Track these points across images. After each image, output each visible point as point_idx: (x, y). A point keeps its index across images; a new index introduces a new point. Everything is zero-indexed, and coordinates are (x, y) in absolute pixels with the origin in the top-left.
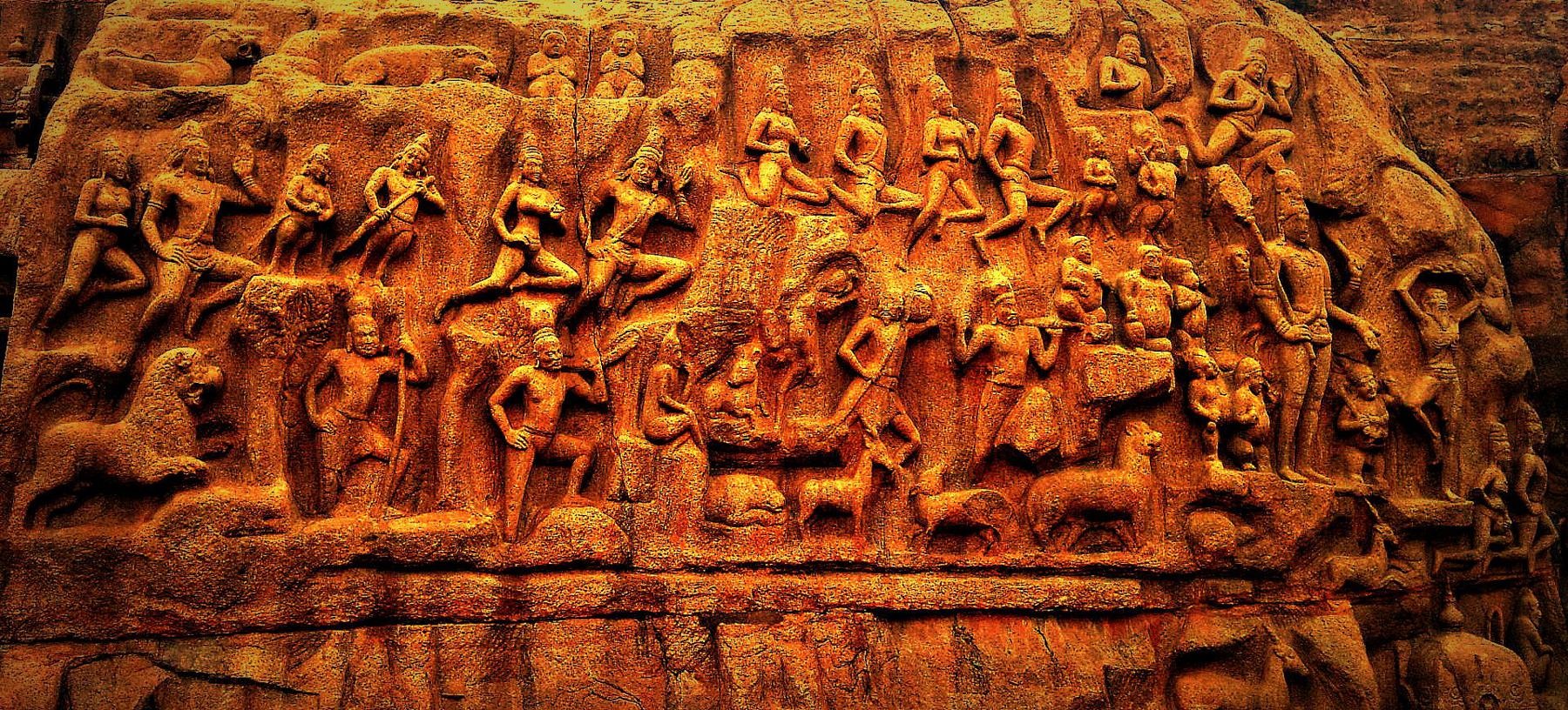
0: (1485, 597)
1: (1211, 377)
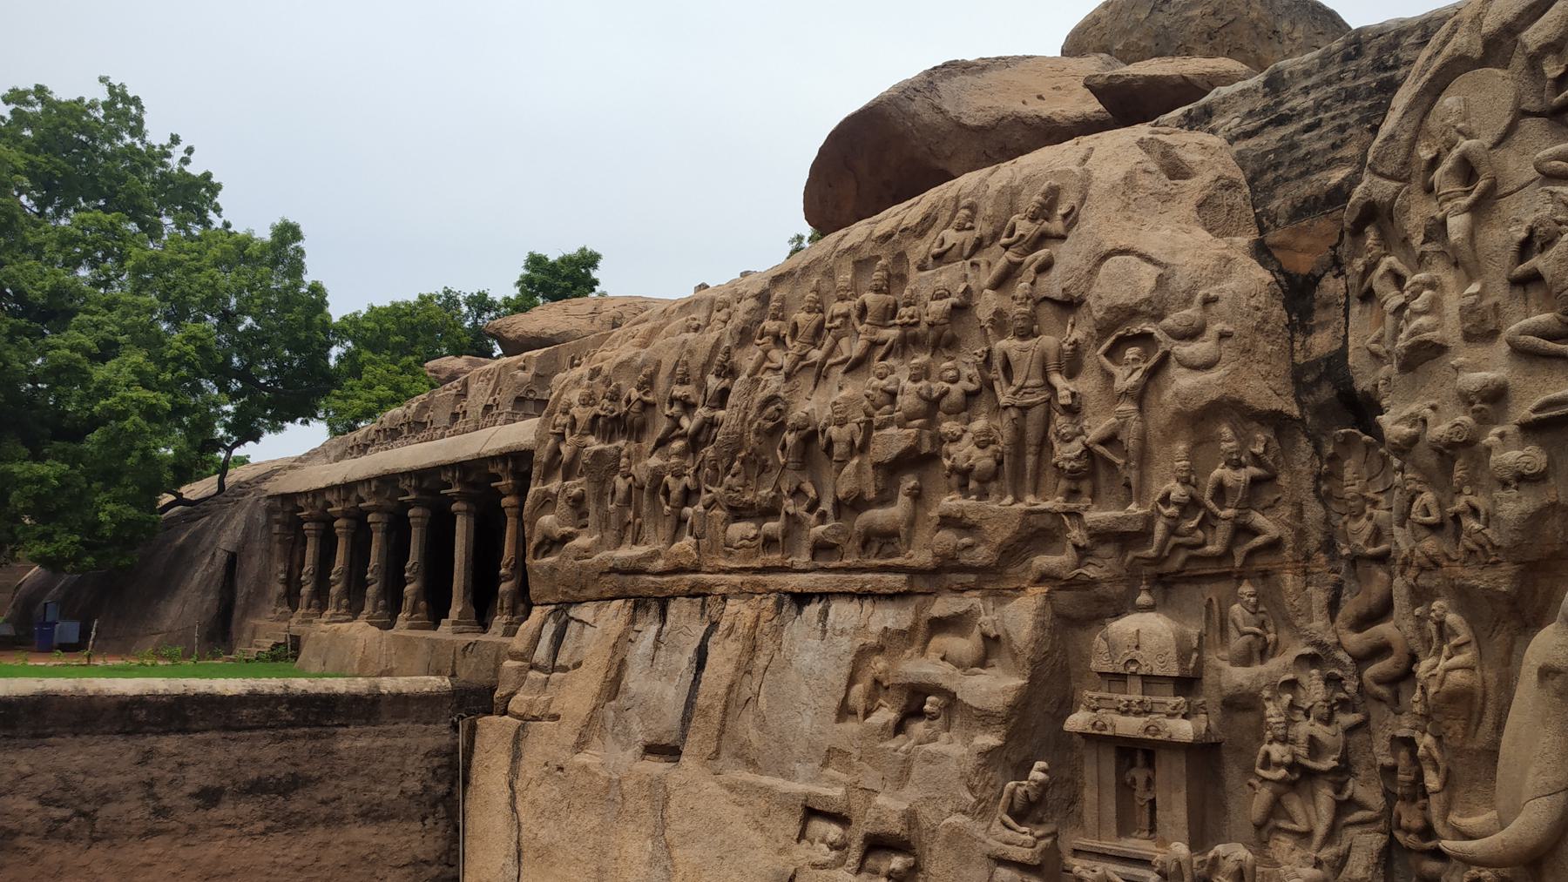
1: (952, 441)
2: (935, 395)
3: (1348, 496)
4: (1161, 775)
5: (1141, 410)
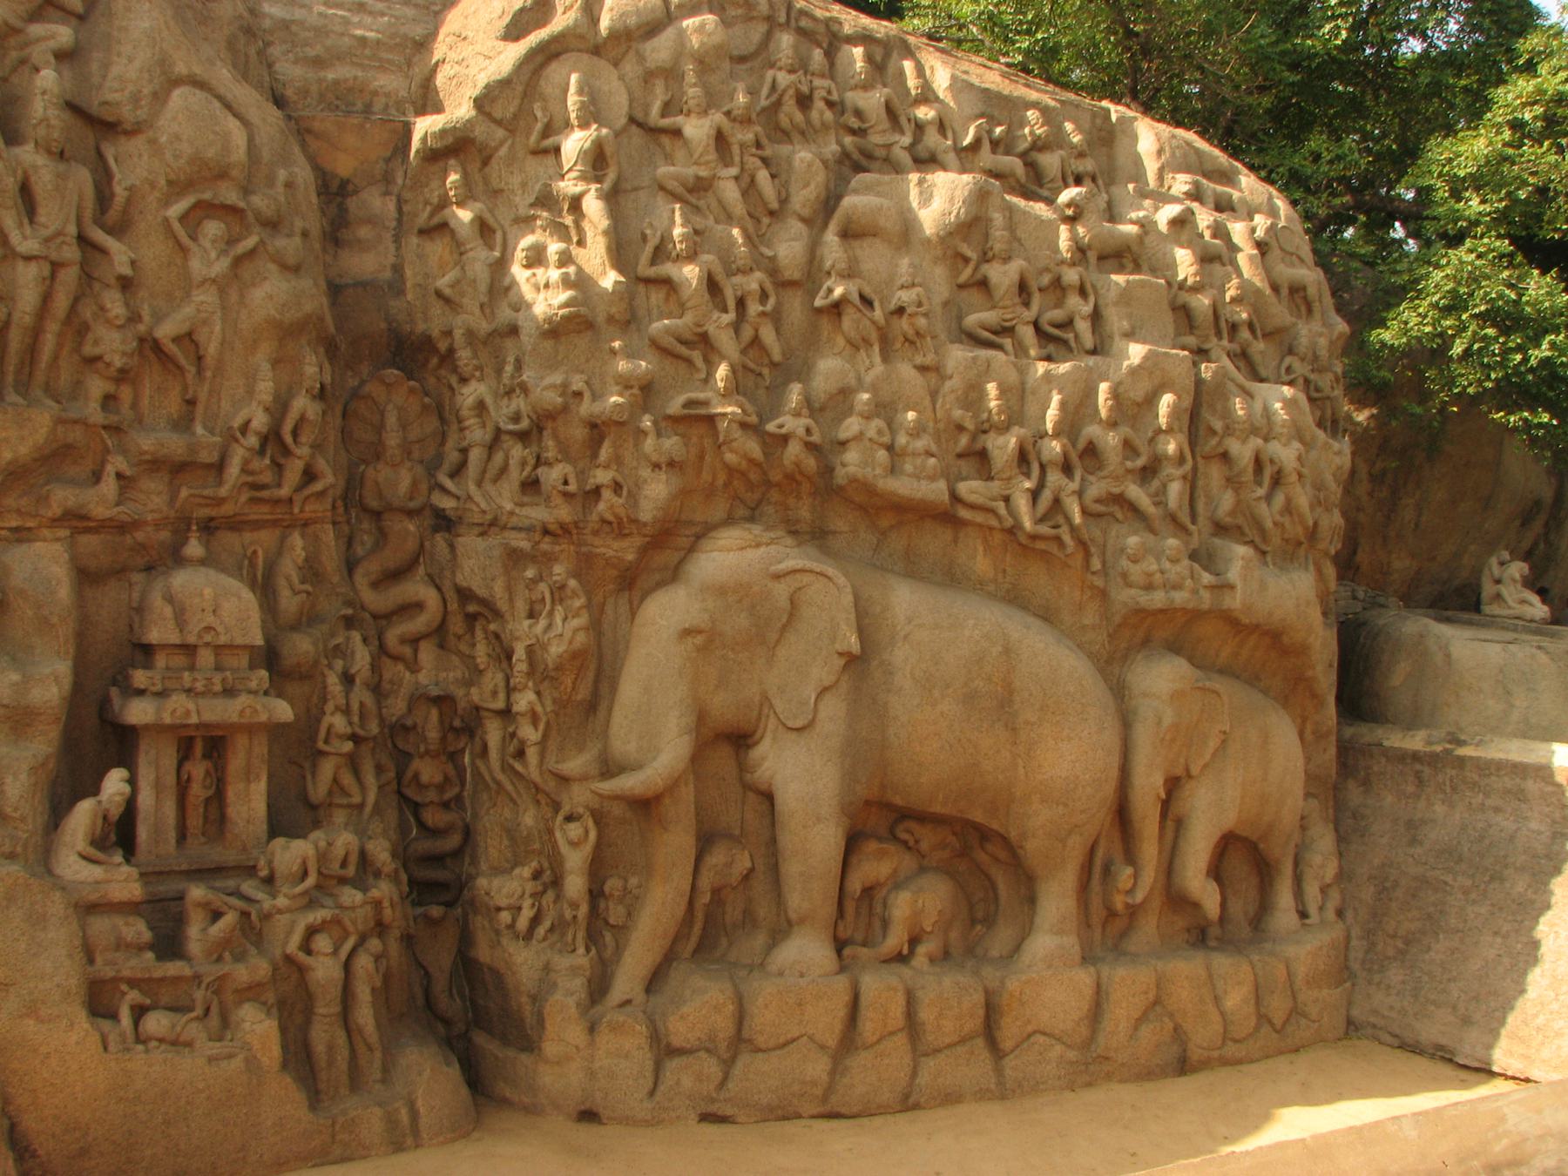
0: (248, 536)
4: (235, 763)
5: (223, 308)
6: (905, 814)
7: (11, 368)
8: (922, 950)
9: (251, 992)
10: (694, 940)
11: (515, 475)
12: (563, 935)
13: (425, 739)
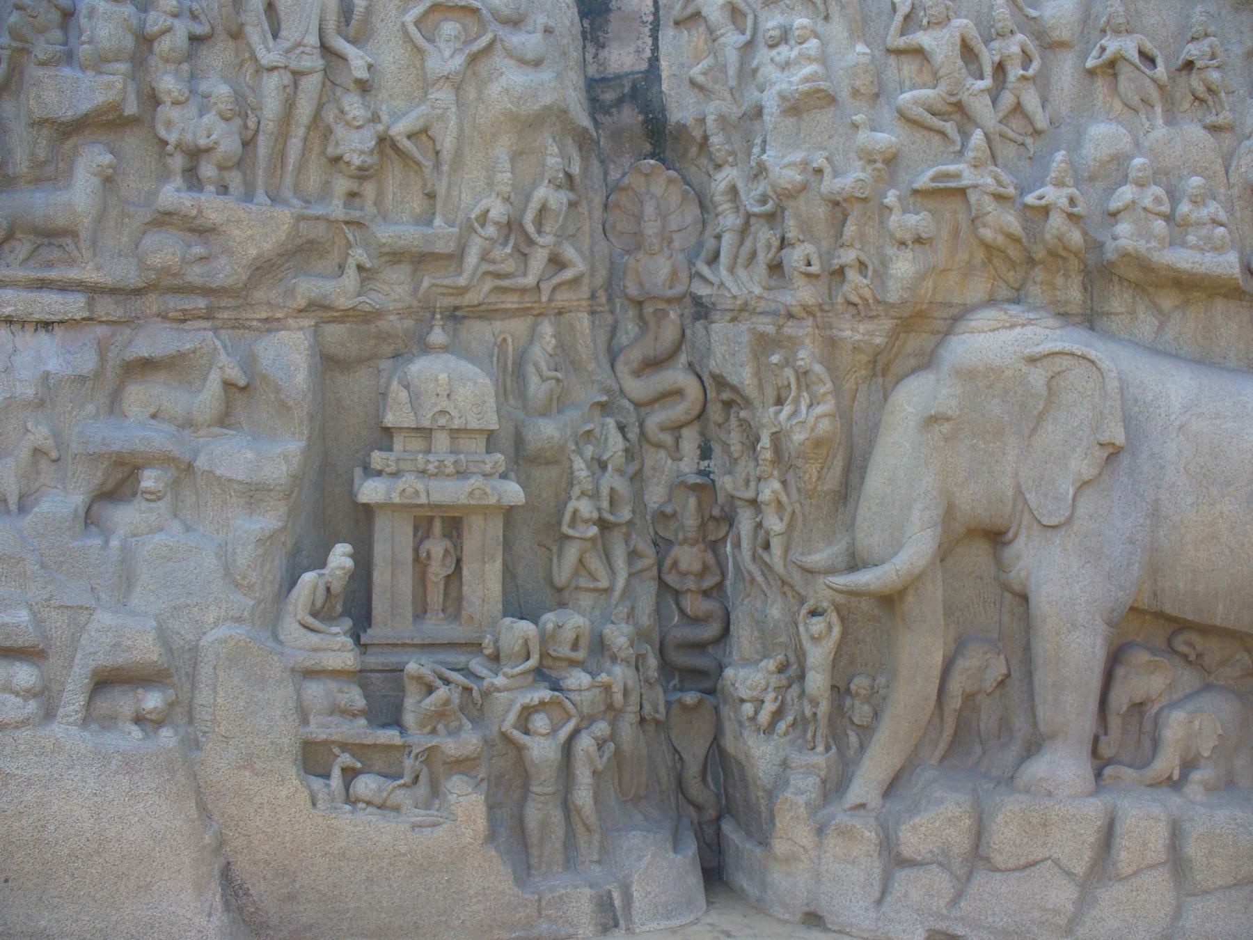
0: (498, 325)
1: (176, 103)
2: (151, 29)
3: (650, 232)
4: (471, 543)
5: (459, 103)
6: (1180, 626)
7: (261, 172)
8: (1196, 776)
9: (462, 765)
10: (942, 746)
11: (762, 259)
12: (805, 732)
13: (683, 526)
